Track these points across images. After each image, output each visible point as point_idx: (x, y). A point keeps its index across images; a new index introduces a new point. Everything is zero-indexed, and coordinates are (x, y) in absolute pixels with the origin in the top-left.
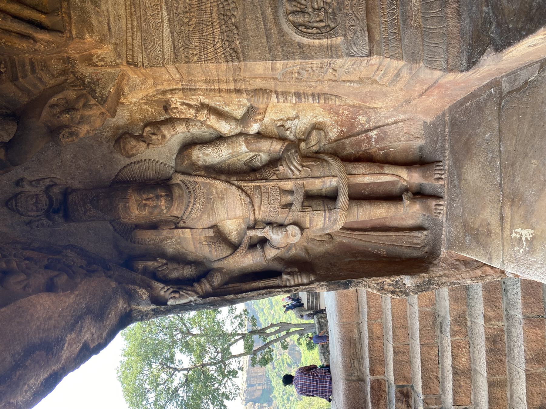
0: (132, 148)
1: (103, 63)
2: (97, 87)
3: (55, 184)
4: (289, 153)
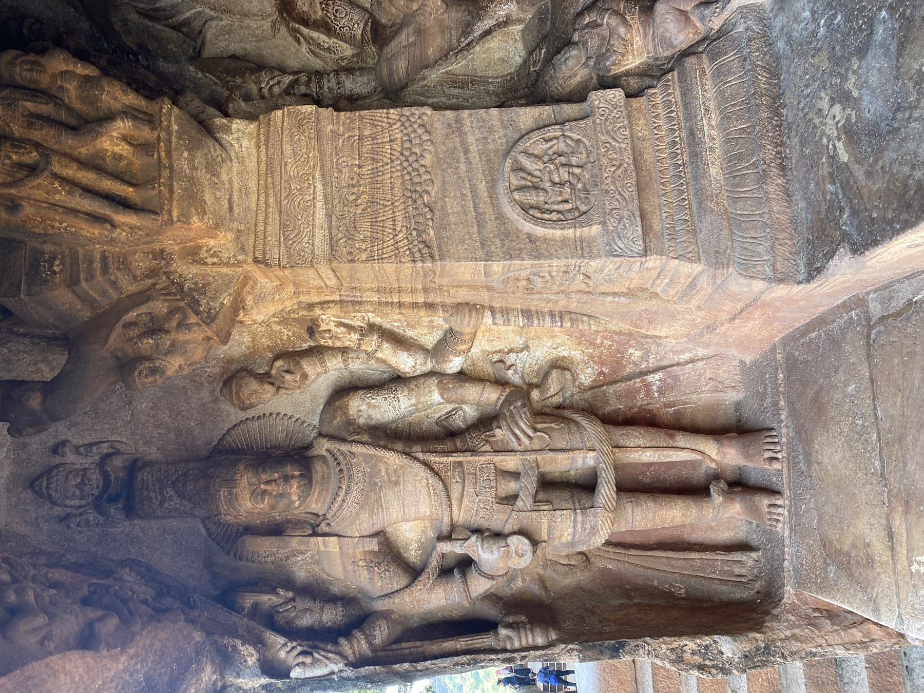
0: (251, 394)
1: (215, 260)
2: (202, 297)
3: (117, 453)
4: (512, 408)
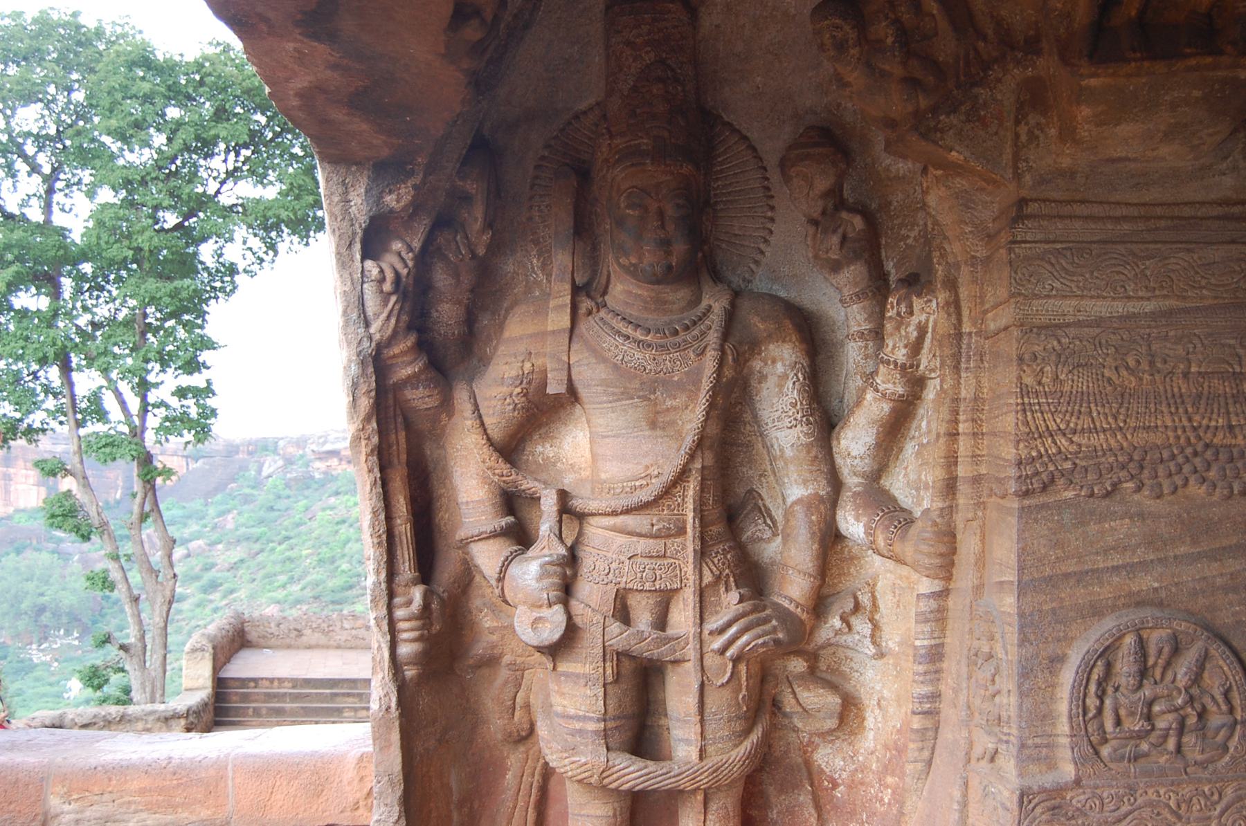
1: (1024, 138)
2: (963, 118)
4: (774, 622)
